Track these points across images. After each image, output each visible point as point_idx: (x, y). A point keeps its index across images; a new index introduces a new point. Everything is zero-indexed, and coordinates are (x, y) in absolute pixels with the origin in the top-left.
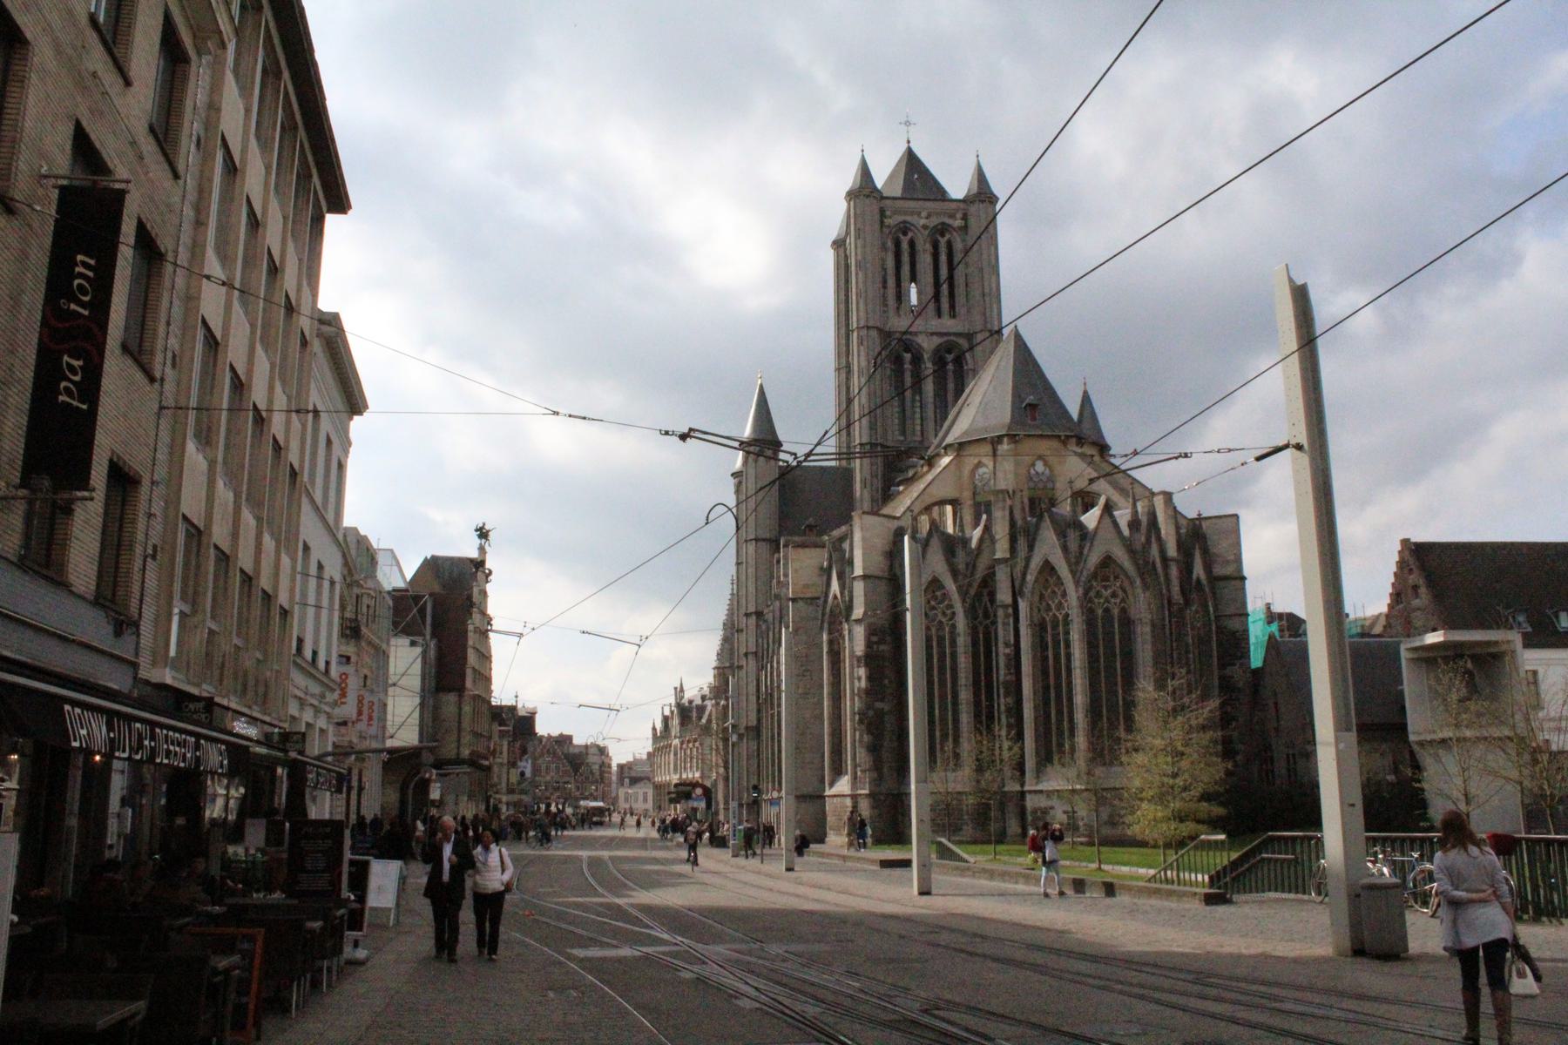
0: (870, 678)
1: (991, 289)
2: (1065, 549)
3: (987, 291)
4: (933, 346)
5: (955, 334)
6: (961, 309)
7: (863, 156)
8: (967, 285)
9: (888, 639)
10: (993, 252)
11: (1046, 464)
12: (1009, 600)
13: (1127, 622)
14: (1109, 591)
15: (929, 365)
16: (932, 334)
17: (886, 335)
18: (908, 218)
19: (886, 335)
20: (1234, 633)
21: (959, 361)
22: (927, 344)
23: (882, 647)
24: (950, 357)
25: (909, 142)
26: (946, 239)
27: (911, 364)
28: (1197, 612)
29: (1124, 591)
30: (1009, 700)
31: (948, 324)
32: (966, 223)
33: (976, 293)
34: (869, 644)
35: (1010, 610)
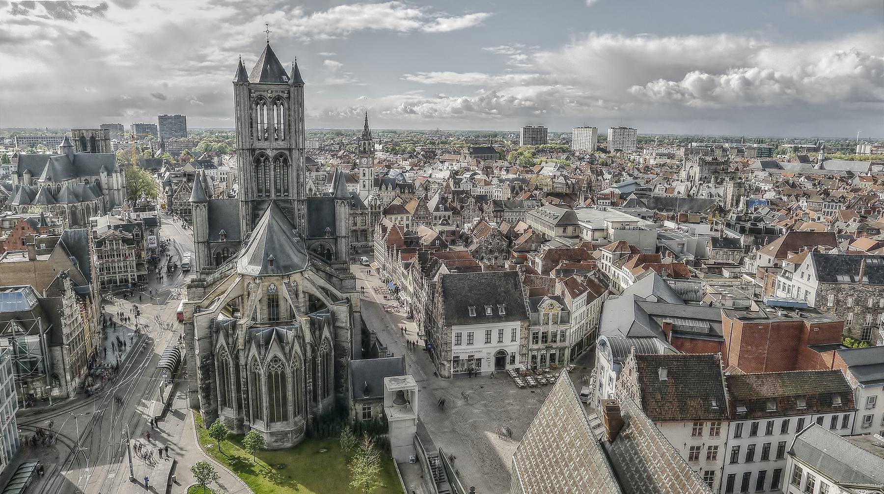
0: (202, 374)
1: (299, 128)
2: (260, 353)
3: (297, 130)
4: (273, 155)
10: (300, 111)
12: (244, 364)
13: (283, 375)
17: (252, 151)
18: (262, 93)
19: (252, 151)
22: (271, 154)
24: (281, 159)
25: (268, 42)
29: (283, 365)
32: (289, 96)
34: (202, 362)
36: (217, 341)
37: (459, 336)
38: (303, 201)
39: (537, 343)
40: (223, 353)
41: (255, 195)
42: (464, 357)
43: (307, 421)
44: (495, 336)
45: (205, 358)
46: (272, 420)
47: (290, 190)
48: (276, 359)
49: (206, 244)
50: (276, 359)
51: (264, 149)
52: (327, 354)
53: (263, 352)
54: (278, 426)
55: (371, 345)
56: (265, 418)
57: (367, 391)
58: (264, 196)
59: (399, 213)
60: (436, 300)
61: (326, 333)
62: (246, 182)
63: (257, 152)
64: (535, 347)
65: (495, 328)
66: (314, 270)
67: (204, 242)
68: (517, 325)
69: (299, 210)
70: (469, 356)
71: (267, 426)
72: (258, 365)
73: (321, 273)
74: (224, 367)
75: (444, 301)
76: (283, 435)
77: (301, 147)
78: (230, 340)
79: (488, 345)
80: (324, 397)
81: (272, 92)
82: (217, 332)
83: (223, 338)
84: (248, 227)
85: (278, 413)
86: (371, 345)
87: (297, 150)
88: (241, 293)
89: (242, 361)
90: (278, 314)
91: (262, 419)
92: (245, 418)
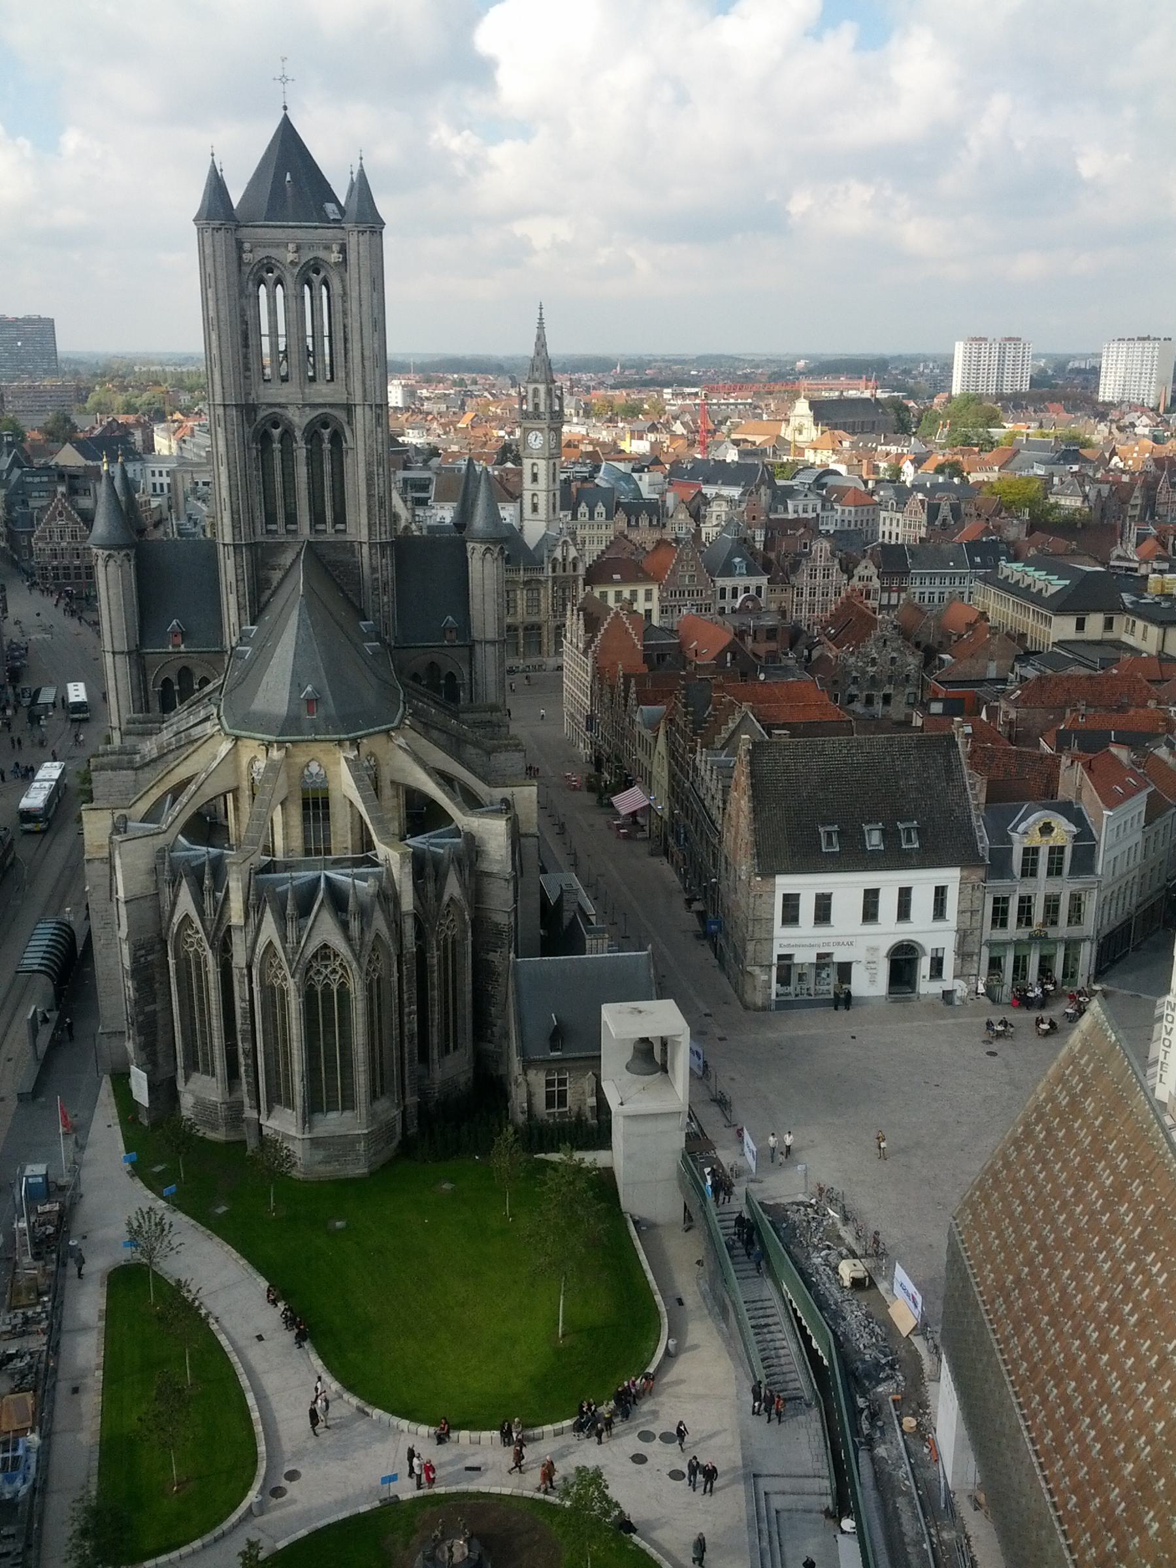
0: (136, 990)
2: (284, 938)
3: (367, 353)
4: (306, 421)
5: (332, 405)
6: (340, 373)
7: (213, 162)
8: (346, 340)
9: (158, 947)
11: (320, 765)
14: (330, 969)
15: (302, 444)
16: (304, 406)
18: (272, 252)
19: (248, 410)
20: (497, 924)
21: (337, 438)
22: (299, 419)
23: (149, 958)
24: (326, 433)
25: (285, 108)
26: (322, 274)
27: (281, 442)
28: (452, 920)
29: (344, 968)
30: (248, 1046)
31: (323, 392)
33: (355, 353)
34: (135, 959)
35: (245, 971)
36: (174, 904)
37: (791, 903)
38: (383, 546)
39: (1004, 924)
40: (189, 936)
41: (259, 531)
42: (805, 957)
43: (404, 1113)
44: (888, 904)
45: (140, 949)
46: (314, 1106)
47: (350, 517)
48: (325, 952)
49: (134, 656)
50: (325, 952)
51: (279, 405)
52: (453, 943)
53: (291, 933)
54: (333, 1123)
55: (566, 922)
56: (298, 1101)
57: (557, 1037)
58: (282, 531)
59: (625, 581)
60: (731, 809)
61: (453, 887)
62: (234, 493)
63: (262, 413)
64: (1000, 935)
65: (888, 882)
66: (419, 726)
67: (129, 653)
68: (950, 877)
69: (374, 570)
70: (819, 956)
71: (304, 1122)
72: (281, 968)
73: (435, 734)
74: (189, 968)
75: (754, 810)
76: (339, 1146)
77: (378, 402)
78: (208, 903)
79: (870, 928)
80: (447, 1051)
81: (298, 249)
82: (175, 884)
83: (190, 898)
84: (242, 612)
85: (332, 1088)
86: (566, 922)
87: (367, 408)
88: (233, 785)
89: (239, 958)
90: (327, 839)
91: (290, 1104)
92: (246, 1100)
